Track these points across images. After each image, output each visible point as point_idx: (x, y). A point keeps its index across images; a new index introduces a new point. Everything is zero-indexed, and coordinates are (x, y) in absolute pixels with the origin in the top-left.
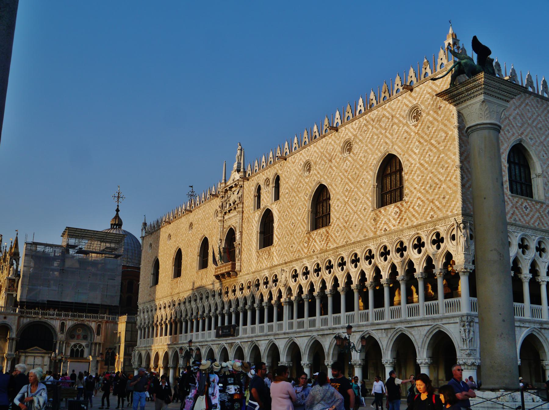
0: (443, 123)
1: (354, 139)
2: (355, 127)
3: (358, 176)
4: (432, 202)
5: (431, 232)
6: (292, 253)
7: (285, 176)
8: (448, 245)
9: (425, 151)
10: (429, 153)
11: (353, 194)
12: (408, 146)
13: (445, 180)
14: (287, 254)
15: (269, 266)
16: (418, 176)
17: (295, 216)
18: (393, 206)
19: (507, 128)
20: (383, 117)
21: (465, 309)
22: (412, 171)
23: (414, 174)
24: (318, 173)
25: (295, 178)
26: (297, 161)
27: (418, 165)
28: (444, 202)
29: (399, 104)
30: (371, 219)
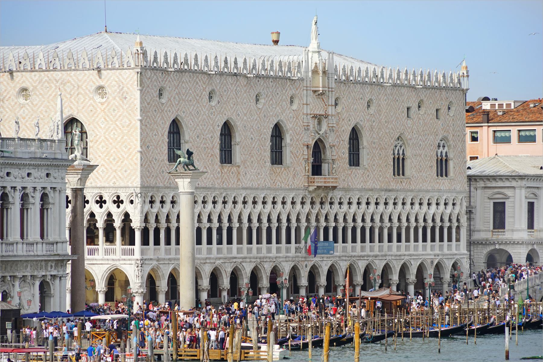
1: (33, 90)
2: (35, 79)
4: (115, 171)
5: (113, 194)
8: (126, 207)
9: (110, 129)
10: (114, 131)
12: (93, 118)
13: (127, 158)
16: (103, 147)
19: (169, 108)
20: (68, 82)
21: (137, 255)
22: (97, 141)
27: (103, 138)
28: (126, 174)
29: (86, 77)
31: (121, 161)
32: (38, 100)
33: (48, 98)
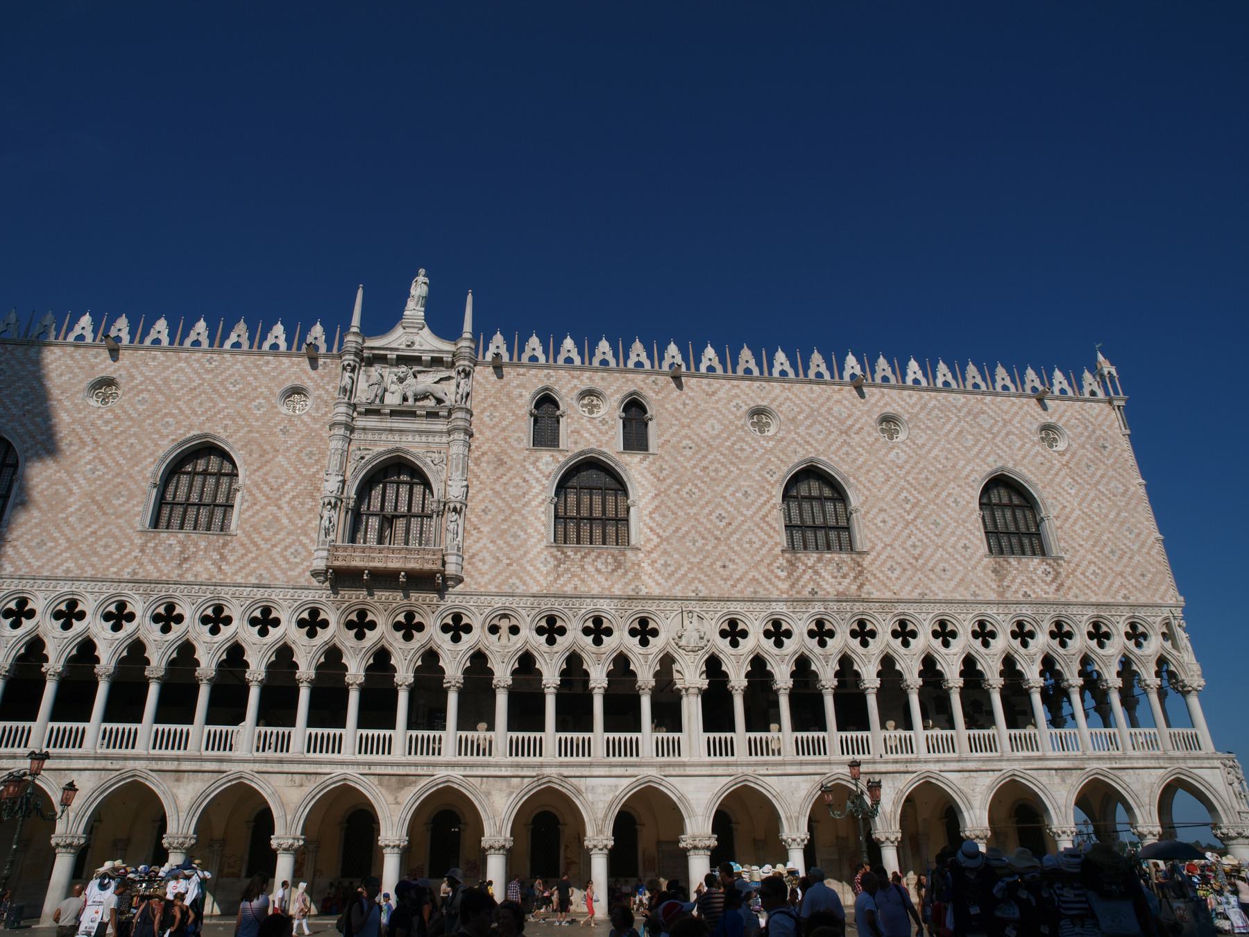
0: (1114, 470)
3: (936, 485)
4: (1121, 574)
6: (726, 580)
7: (677, 409)
11: (927, 512)
15: (617, 591)
16: (1083, 529)
17: (732, 504)
18: (1036, 561)
23: (1075, 523)
24: (808, 443)
25: (718, 427)
26: (721, 394)
27: (1077, 512)
29: (1015, 409)
30: (986, 568)
31: (1128, 555)
32: (925, 437)
33: (947, 434)
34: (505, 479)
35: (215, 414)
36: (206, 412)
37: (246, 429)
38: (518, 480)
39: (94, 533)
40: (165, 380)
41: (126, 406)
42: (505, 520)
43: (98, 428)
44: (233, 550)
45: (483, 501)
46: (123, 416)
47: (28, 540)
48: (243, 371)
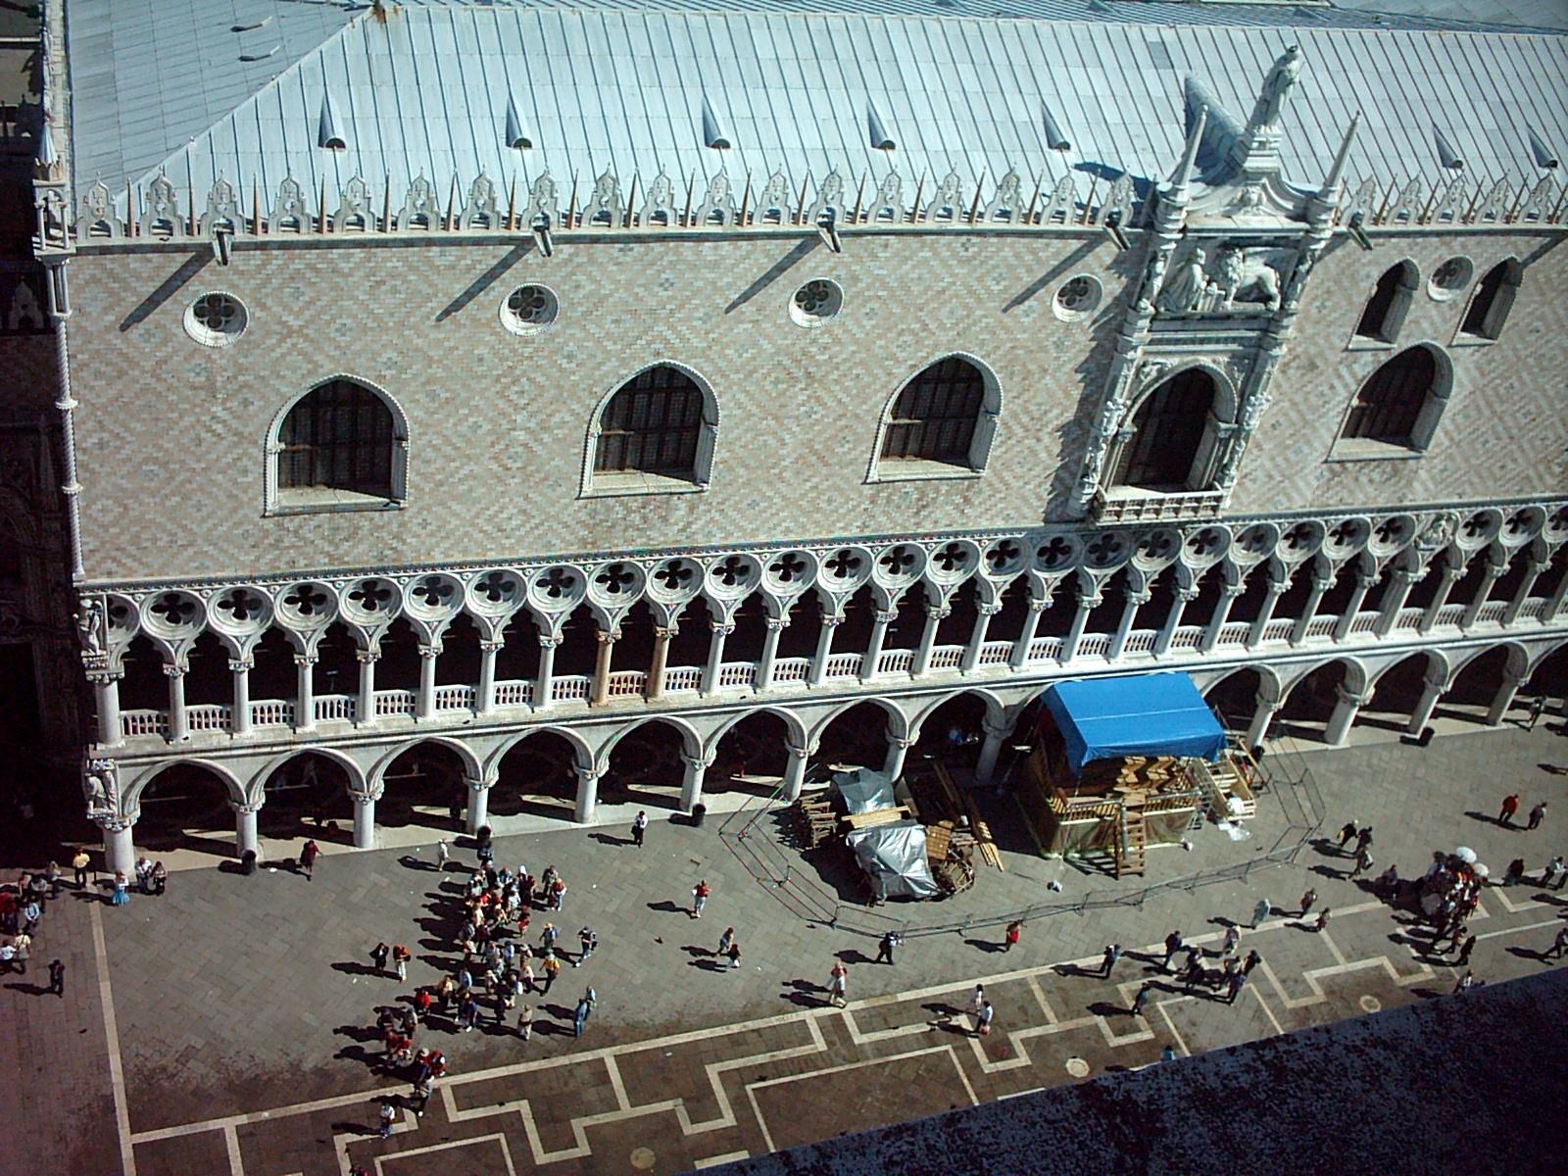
6: (1496, 480)
7: (1549, 280)
14: (1476, 480)
34: (1310, 387)
35: (969, 327)
36: (957, 324)
37: (1009, 345)
38: (1325, 388)
39: (816, 487)
40: (901, 280)
41: (850, 324)
42: (1291, 435)
43: (813, 357)
44: (980, 491)
45: (1275, 415)
46: (844, 337)
47: (737, 503)
48: (1013, 261)
